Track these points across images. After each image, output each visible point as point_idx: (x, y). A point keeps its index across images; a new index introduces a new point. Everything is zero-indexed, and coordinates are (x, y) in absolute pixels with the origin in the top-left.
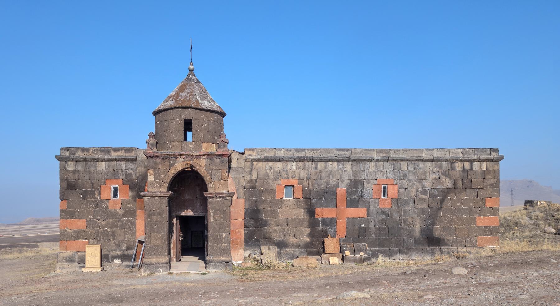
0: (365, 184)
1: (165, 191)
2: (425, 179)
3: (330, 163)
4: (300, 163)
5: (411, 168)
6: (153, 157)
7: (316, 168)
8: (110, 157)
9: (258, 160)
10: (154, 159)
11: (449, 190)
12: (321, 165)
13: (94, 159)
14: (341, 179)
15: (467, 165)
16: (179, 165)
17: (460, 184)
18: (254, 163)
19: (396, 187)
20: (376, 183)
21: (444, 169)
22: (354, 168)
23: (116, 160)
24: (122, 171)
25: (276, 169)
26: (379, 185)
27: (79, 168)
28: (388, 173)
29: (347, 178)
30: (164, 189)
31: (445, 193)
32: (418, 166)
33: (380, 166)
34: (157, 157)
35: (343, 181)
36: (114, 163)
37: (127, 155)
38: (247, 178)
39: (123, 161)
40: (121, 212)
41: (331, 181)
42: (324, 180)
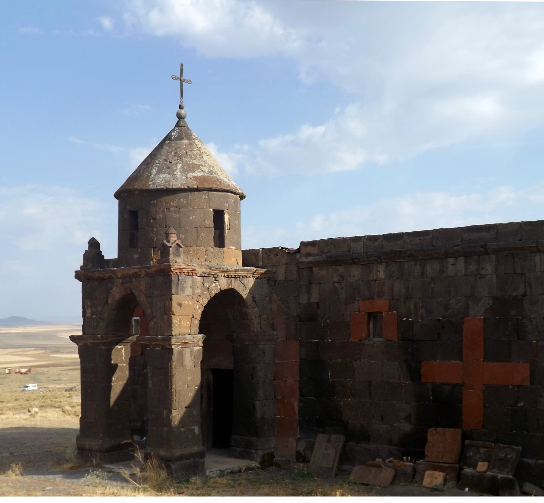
3: (451, 260)
7: (423, 274)
9: (317, 264)
18: (314, 269)
38: (304, 300)
41: (453, 301)
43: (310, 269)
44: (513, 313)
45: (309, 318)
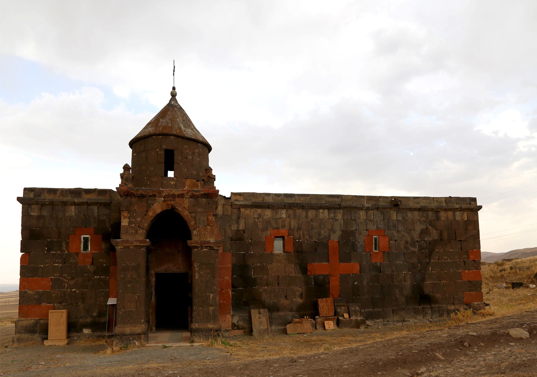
0: (357, 235)
1: (142, 238)
2: (414, 230)
3: (321, 211)
4: (291, 210)
5: (400, 218)
6: (127, 195)
7: (307, 216)
8: (81, 200)
9: (245, 206)
10: (129, 198)
11: (435, 241)
12: (311, 214)
13: (62, 202)
14: (332, 230)
16: (158, 207)
17: (445, 235)
18: (241, 209)
19: (387, 239)
20: (367, 235)
21: (430, 219)
22: (346, 217)
23: (88, 204)
24: (94, 218)
25: (265, 217)
26: (370, 236)
27: (45, 213)
28: (378, 223)
29: (338, 228)
31: (433, 244)
32: (407, 216)
33: (370, 215)
34: (132, 195)
35: (334, 232)
36: (85, 207)
37: (100, 198)
38: (234, 227)
39: (96, 205)
41: (322, 232)
42: (316, 231)
43: (239, 209)
44: (351, 238)
45: (238, 238)
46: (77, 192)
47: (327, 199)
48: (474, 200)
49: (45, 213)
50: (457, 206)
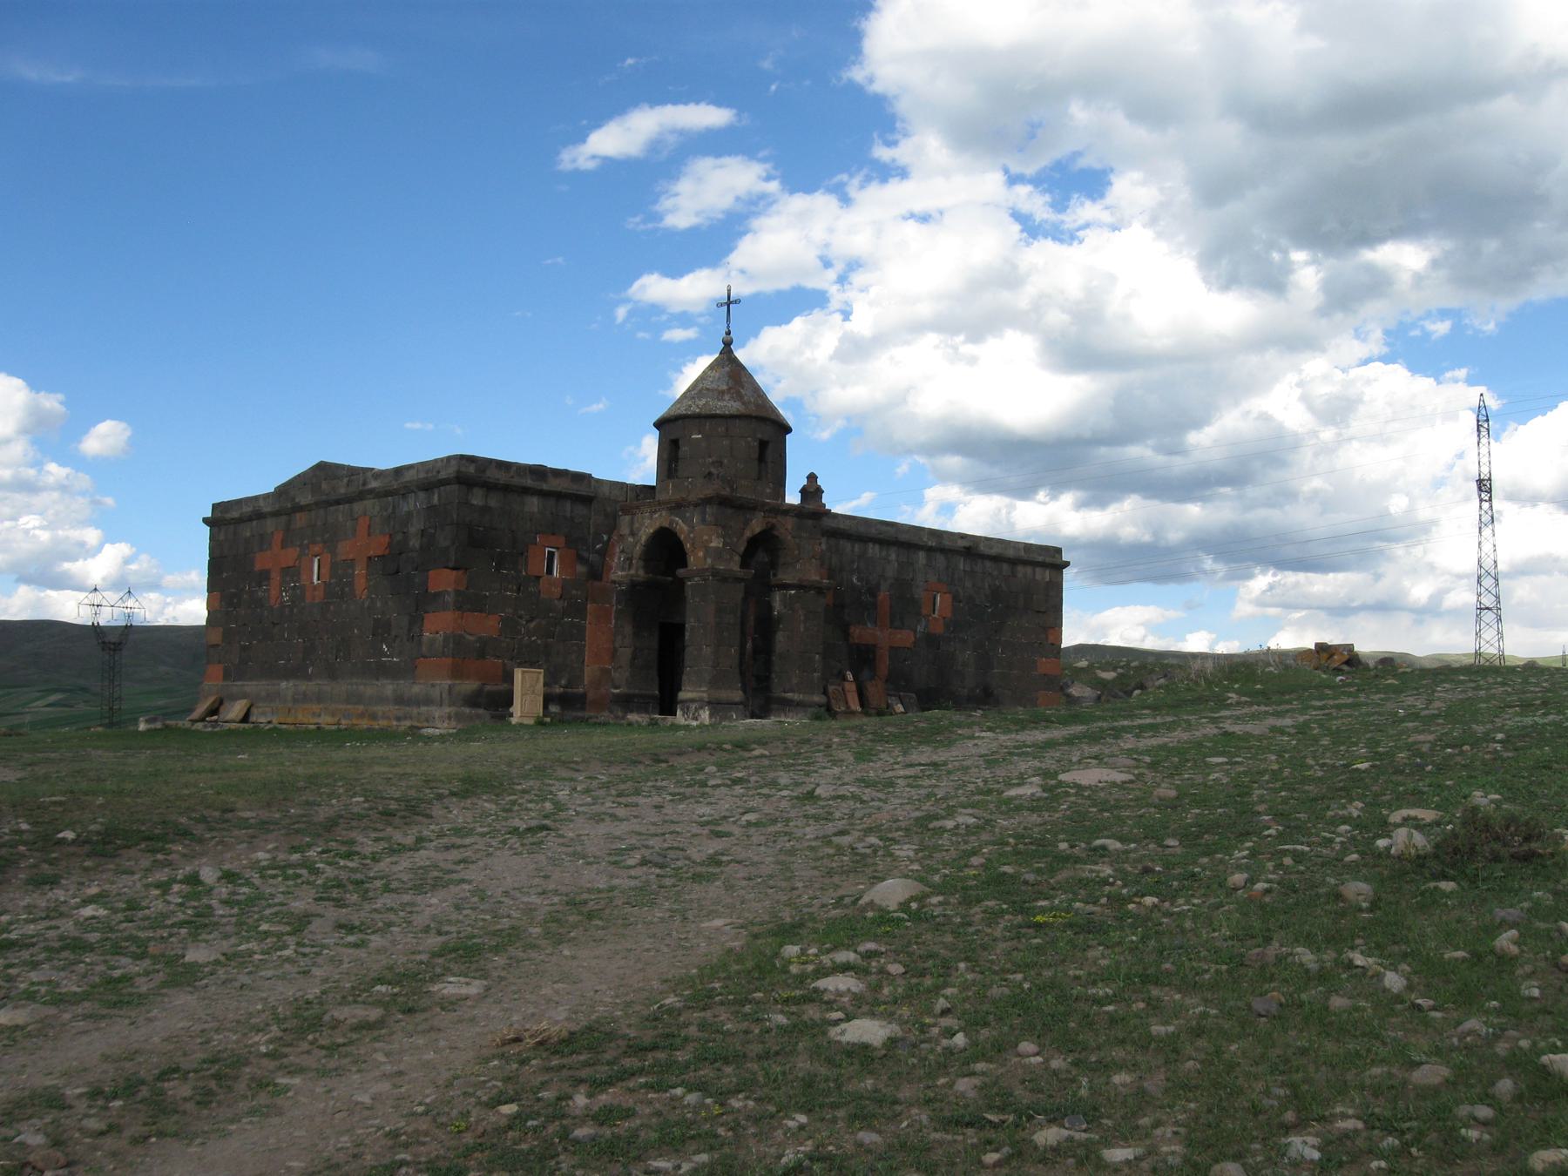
15: (1029, 570)
30: (735, 566)
40: (560, 604)
46: (539, 472)
47: (884, 528)
48: (1058, 551)
49: (493, 503)
50: (1040, 559)
